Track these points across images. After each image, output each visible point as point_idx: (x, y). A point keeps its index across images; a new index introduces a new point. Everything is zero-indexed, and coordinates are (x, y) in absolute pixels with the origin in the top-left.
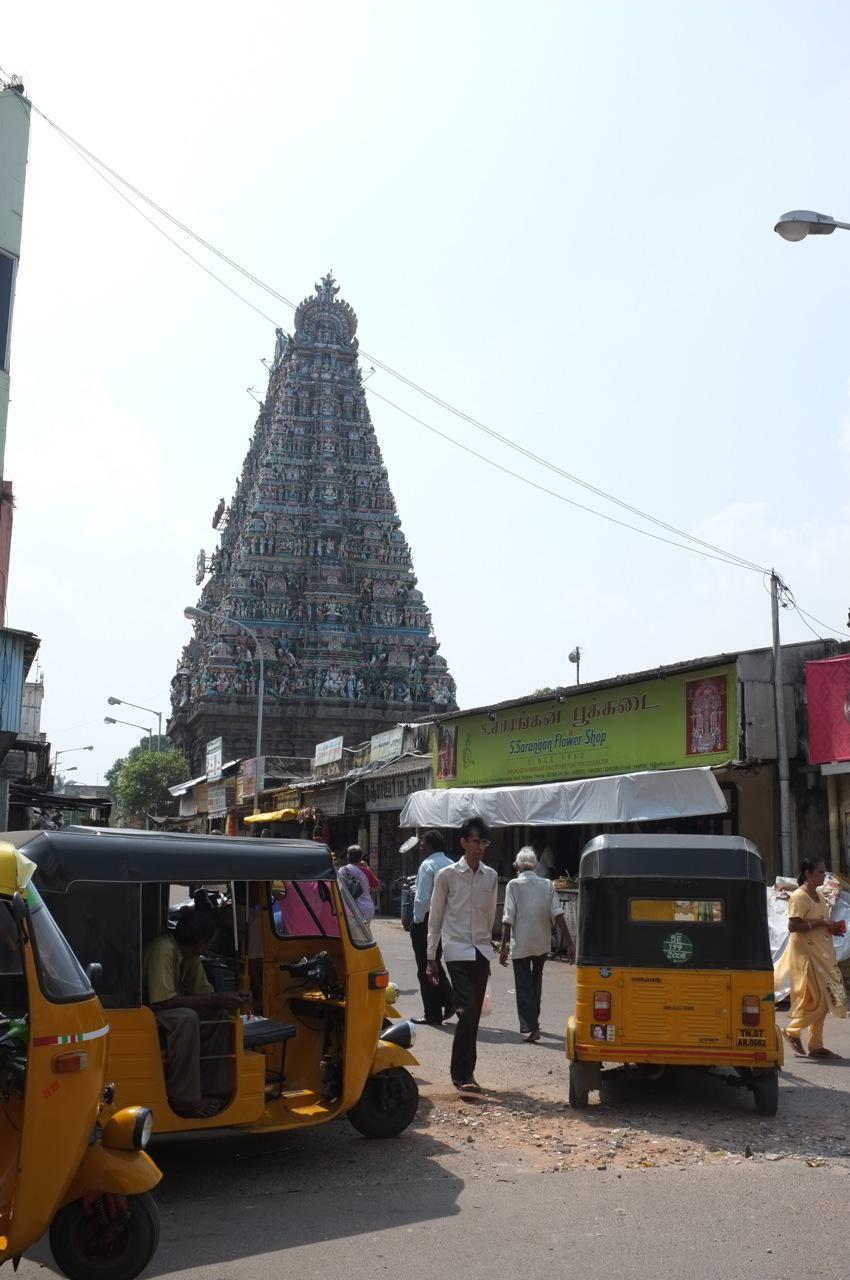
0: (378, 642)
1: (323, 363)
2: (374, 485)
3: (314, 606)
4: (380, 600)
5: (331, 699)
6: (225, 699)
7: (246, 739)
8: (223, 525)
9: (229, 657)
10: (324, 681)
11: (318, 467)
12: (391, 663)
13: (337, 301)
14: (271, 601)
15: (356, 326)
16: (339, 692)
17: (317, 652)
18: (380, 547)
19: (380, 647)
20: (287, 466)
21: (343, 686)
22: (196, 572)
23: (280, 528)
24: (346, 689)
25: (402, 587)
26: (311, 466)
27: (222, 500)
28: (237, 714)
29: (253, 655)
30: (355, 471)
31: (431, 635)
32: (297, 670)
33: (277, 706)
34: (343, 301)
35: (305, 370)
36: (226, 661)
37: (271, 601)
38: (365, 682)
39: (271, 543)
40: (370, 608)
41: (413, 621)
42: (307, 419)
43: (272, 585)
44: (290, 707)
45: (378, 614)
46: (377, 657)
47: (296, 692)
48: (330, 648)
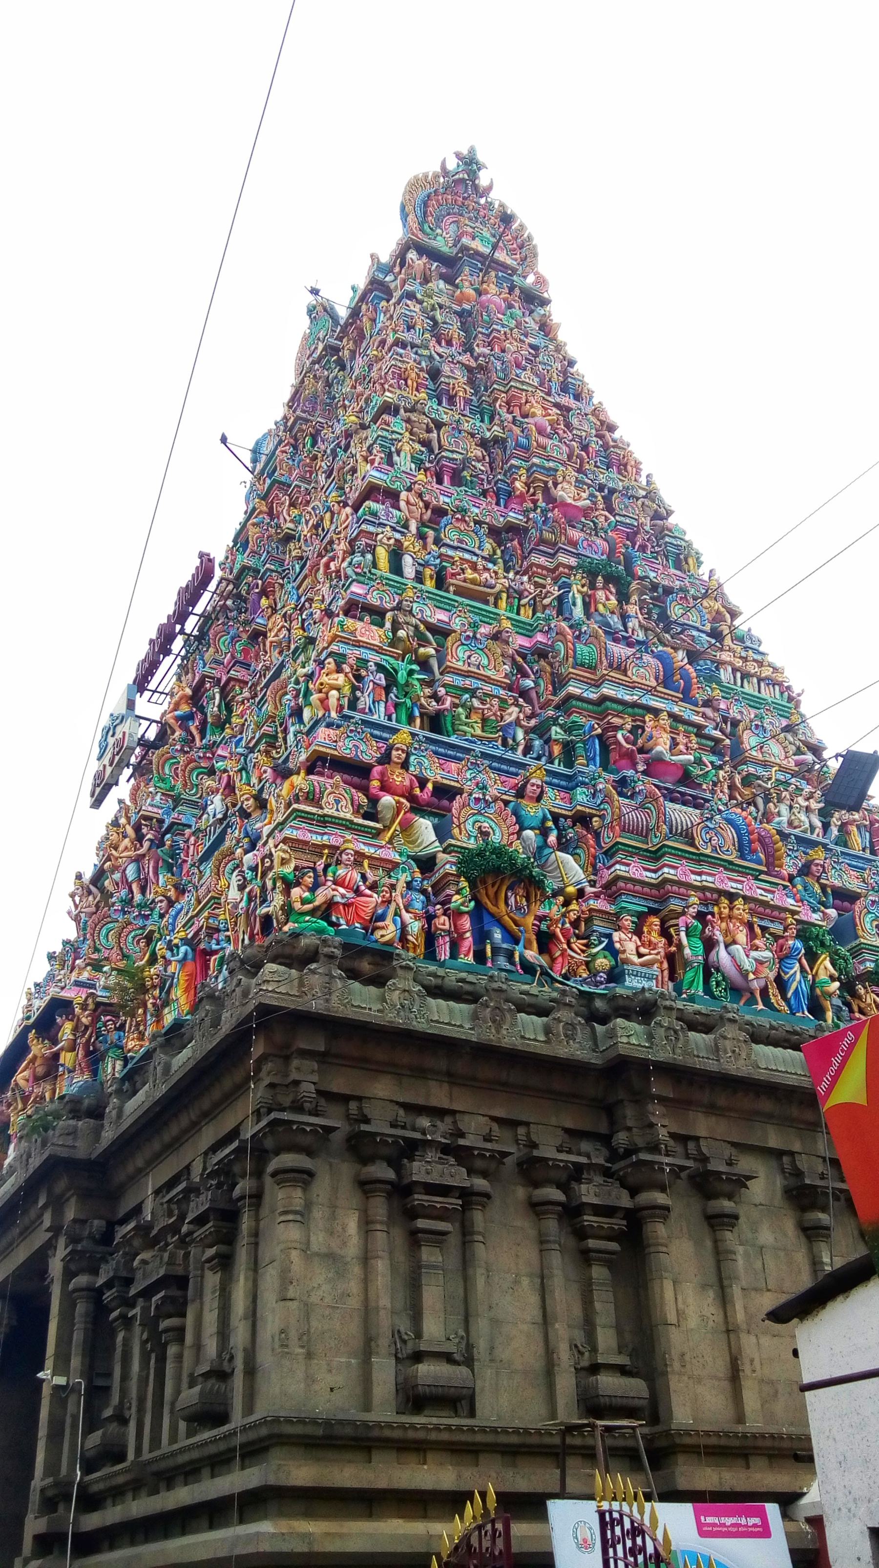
7: (446, 1150)
16: (764, 992)
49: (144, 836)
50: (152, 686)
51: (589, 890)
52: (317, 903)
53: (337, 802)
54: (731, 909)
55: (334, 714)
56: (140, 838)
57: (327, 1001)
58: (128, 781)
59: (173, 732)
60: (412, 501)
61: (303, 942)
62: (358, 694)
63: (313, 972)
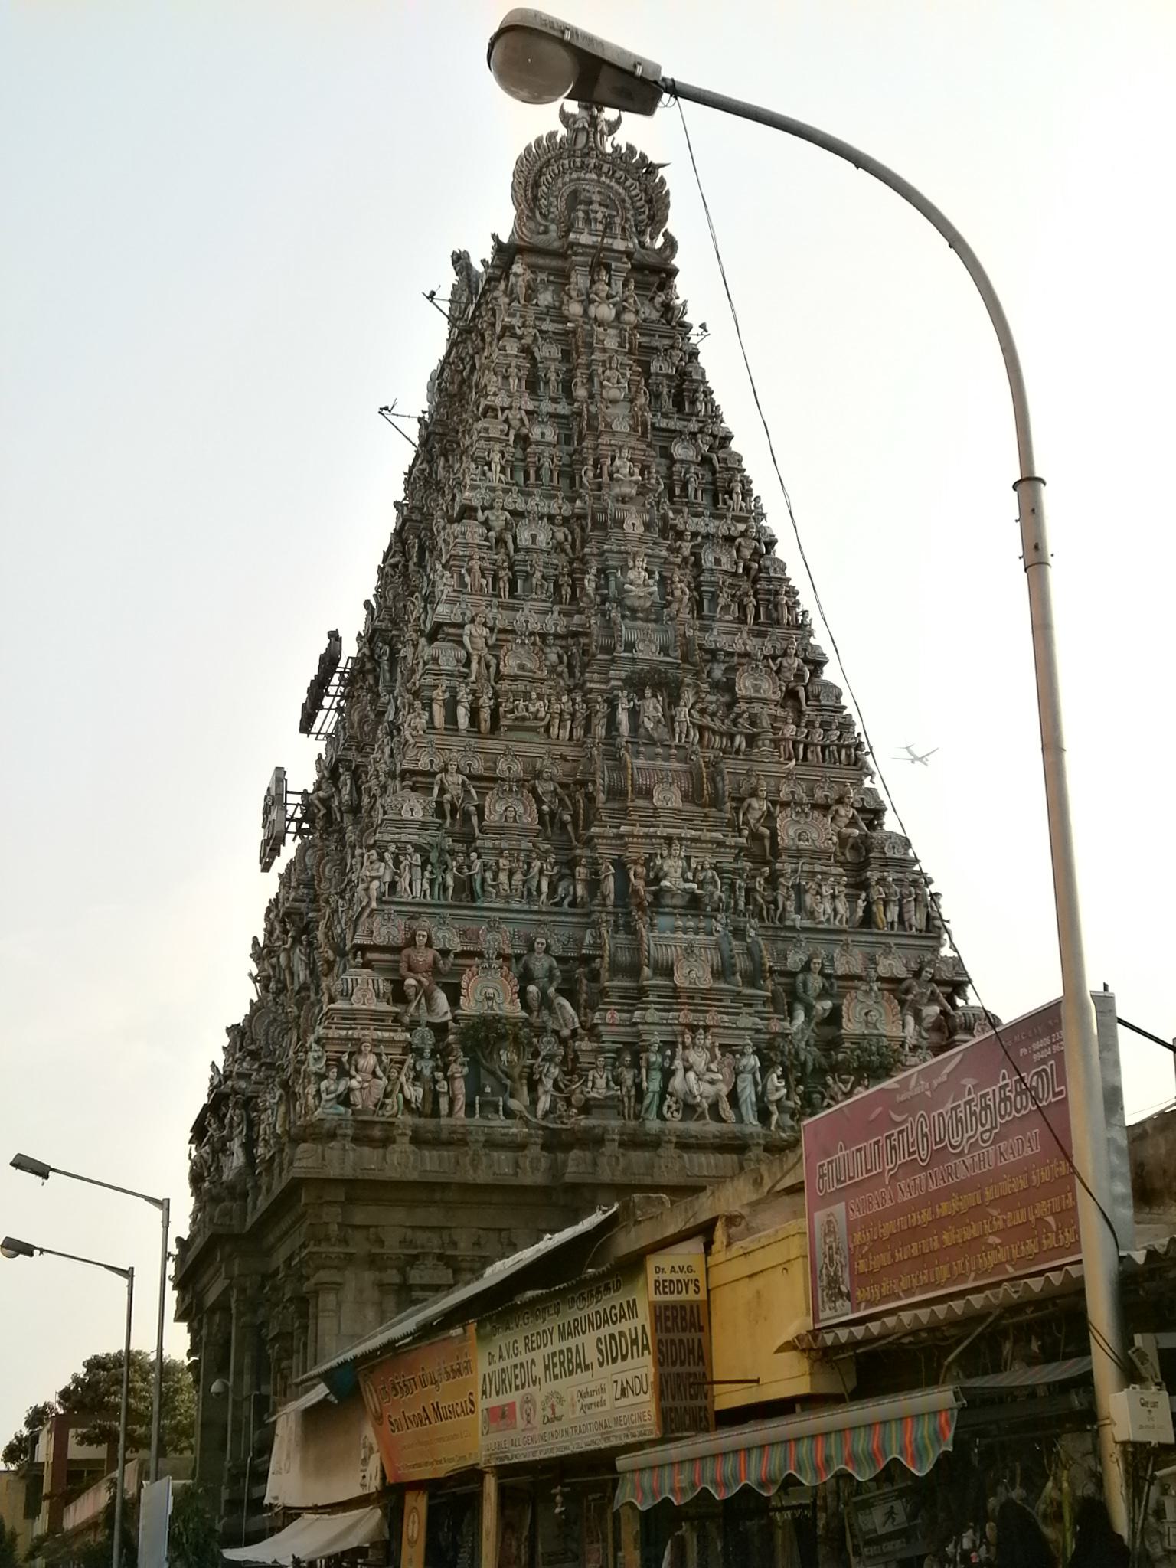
0: (807, 968)
1: (593, 282)
2: (747, 569)
3: (621, 866)
4: (798, 854)
5: (693, 1127)
6: (377, 1132)
7: (440, 1257)
8: (326, 720)
9: (383, 1007)
10: (668, 1074)
11: (600, 517)
12: (851, 1026)
13: (617, 149)
14: (499, 852)
15: (667, 206)
16: (714, 1106)
17: (642, 991)
18: (785, 720)
19: (816, 982)
20: (517, 514)
21: (724, 1090)
22: (259, 835)
23: (509, 666)
24: (733, 1097)
25: (852, 823)
26: (581, 517)
27: (334, 636)
28: (414, 1176)
29: (454, 1002)
30: (694, 535)
31: (946, 951)
32: (585, 1045)
33: (534, 1151)
34: (630, 148)
35: (546, 298)
36: (375, 1017)
37: (499, 852)
38: (784, 1076)
39: (486, 701)
40: (772, 881)
41: (893, 913)
42: (563, 408)
43: (495, 811)
44: (575, 1153)
45: (799, 890)
46: (809, 1009)
47: (586, 1108)
48: (679, 980)
49: (288, 932)
50: (315, 728)
51: (580, 1031)
52: (339, 1092)
53: (364, 996)
54: (693, 1039)
55: (374, 905)
56: (285, 932)
57: (342, 1168)
58: (294, 840)
59: (319, 811)
60: (474, 633)
61: (327, 1125)
62: (397, 878)
63: (331, 1148)
